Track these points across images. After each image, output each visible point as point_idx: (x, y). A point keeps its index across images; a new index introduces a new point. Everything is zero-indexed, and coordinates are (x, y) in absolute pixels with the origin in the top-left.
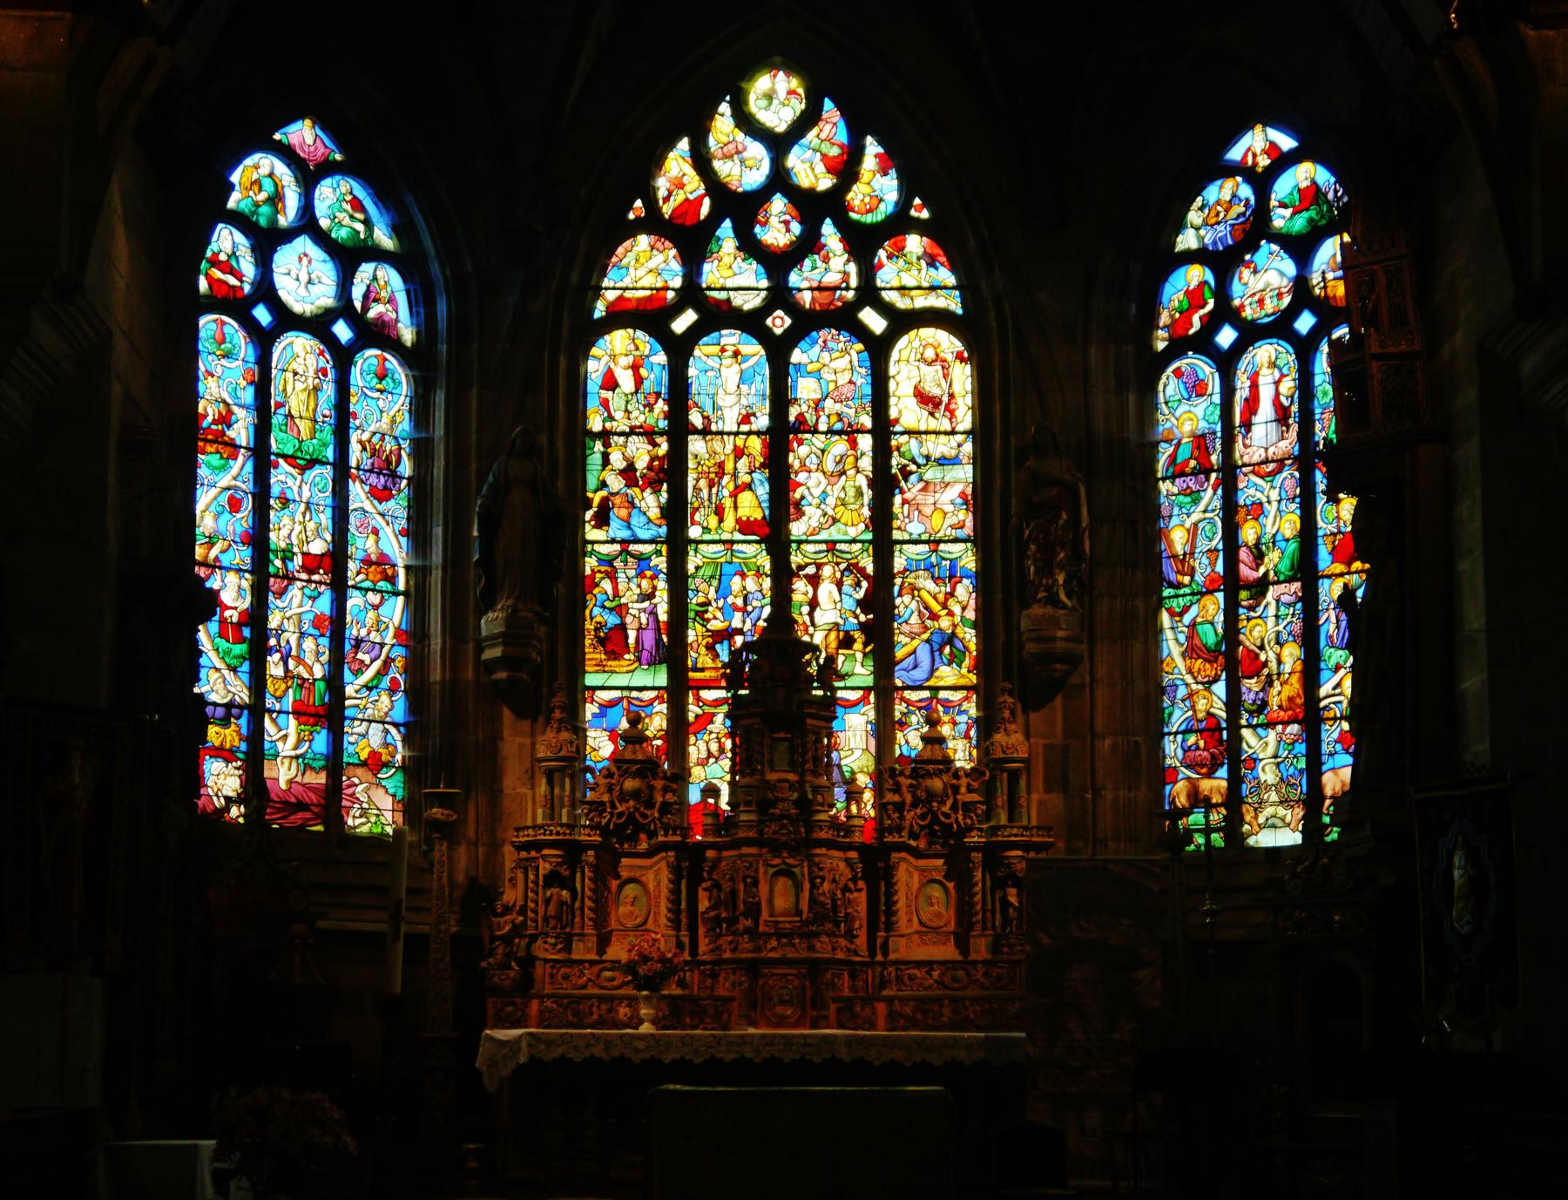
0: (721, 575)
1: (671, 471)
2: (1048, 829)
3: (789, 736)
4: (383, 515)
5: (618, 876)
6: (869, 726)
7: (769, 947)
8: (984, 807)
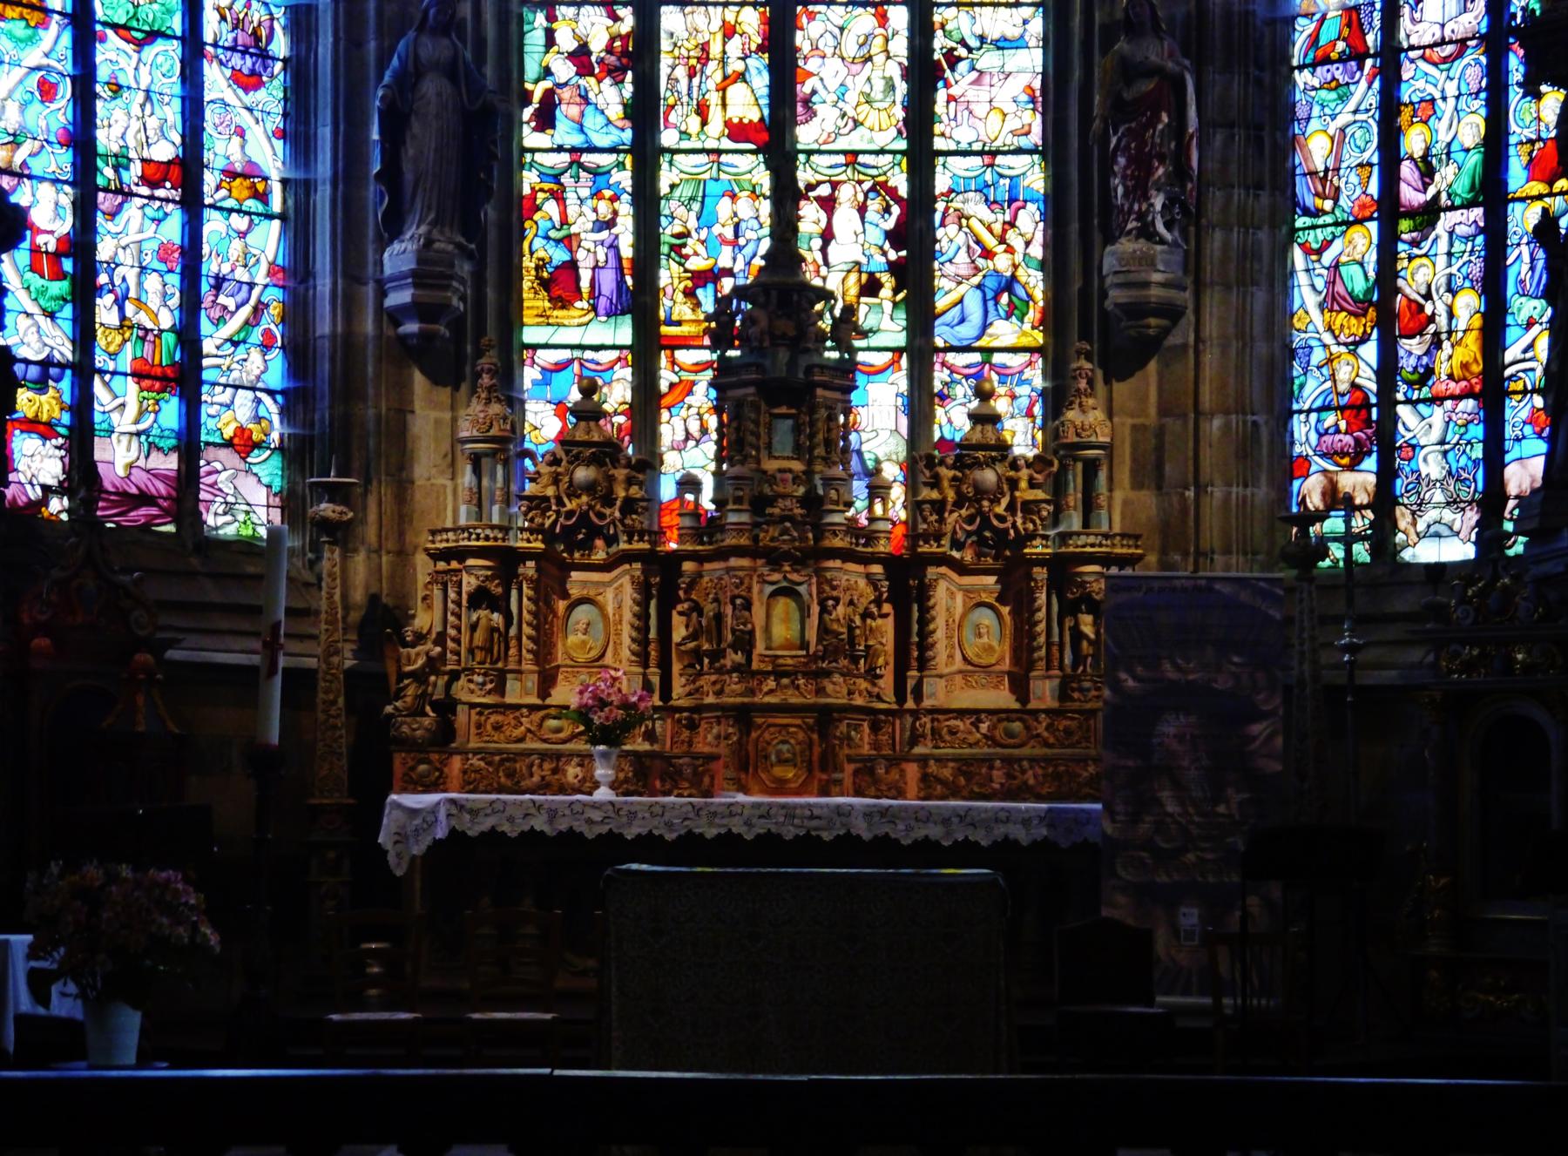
0: (704, 196)
2: (1137, 537)
3: (793, 411)
4: (250, 110)
5: (565, 595)
6: (900, 400)
7: (766, 689)
8: (1051, 508)
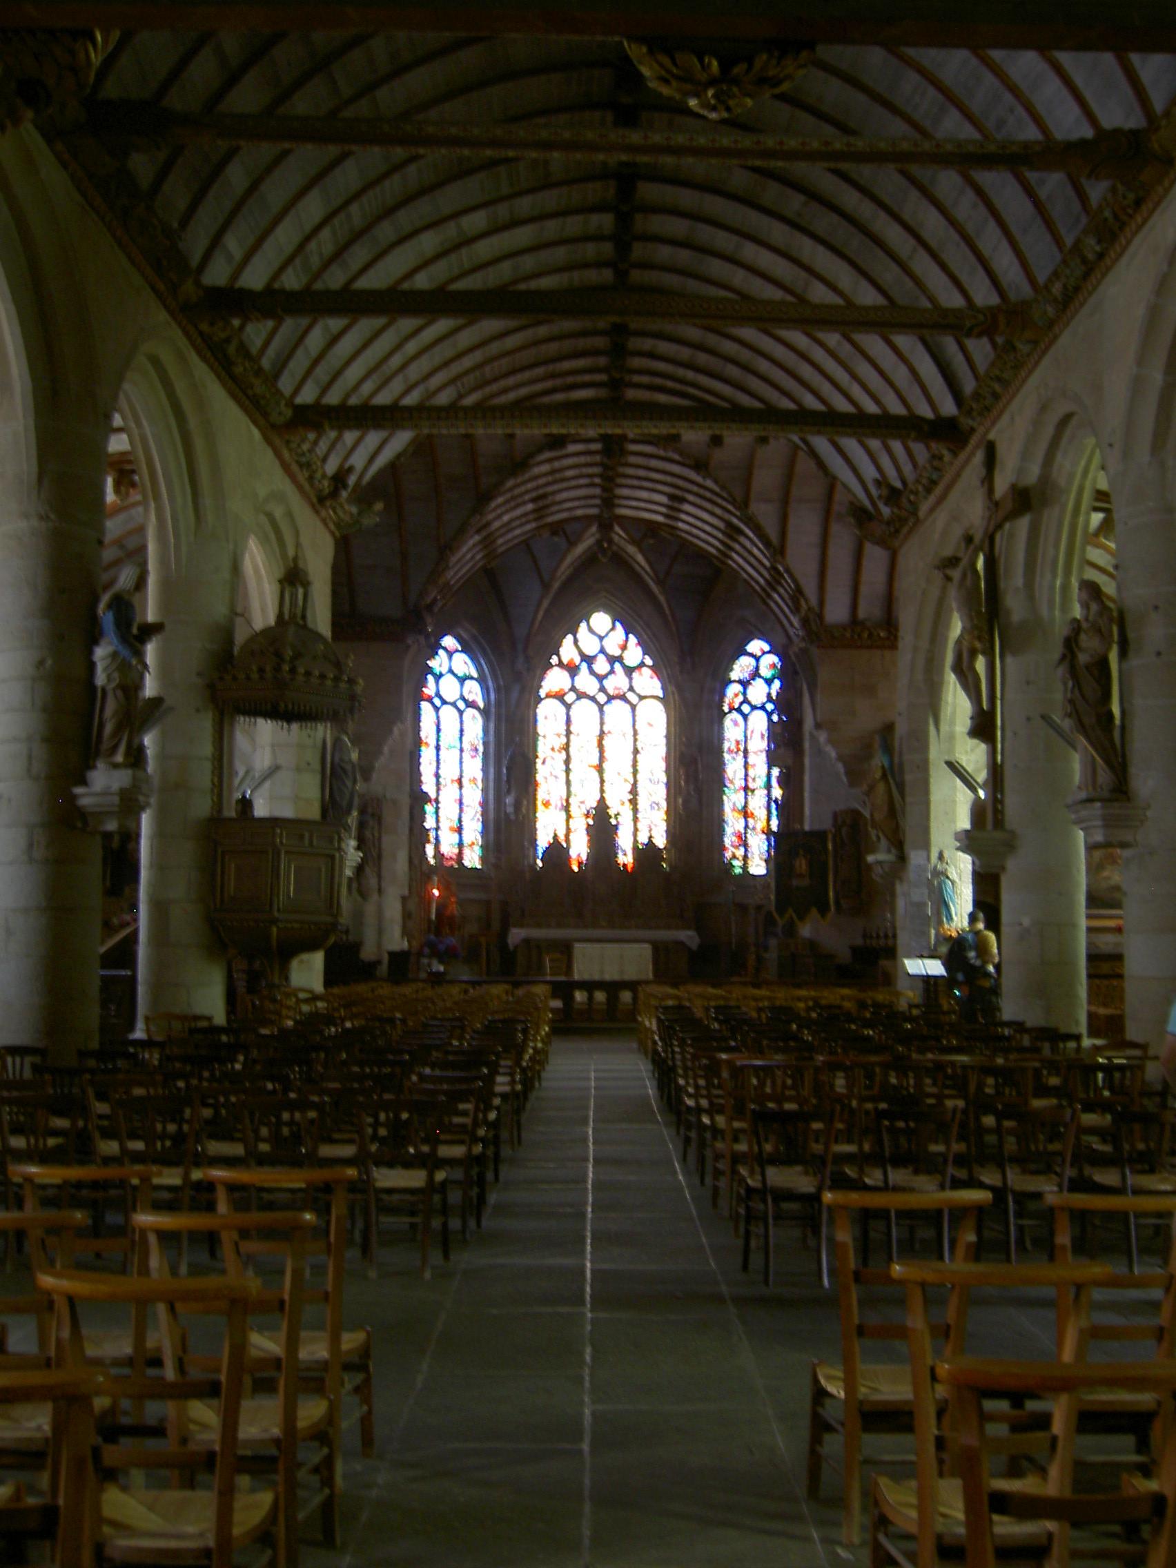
1: (566, 748)
